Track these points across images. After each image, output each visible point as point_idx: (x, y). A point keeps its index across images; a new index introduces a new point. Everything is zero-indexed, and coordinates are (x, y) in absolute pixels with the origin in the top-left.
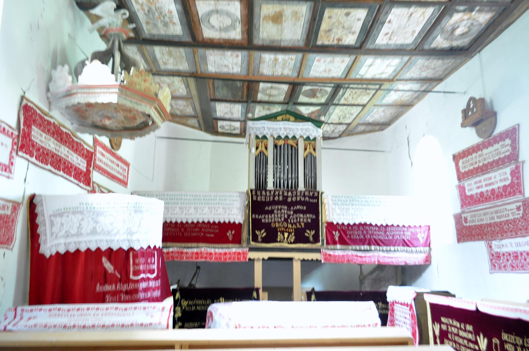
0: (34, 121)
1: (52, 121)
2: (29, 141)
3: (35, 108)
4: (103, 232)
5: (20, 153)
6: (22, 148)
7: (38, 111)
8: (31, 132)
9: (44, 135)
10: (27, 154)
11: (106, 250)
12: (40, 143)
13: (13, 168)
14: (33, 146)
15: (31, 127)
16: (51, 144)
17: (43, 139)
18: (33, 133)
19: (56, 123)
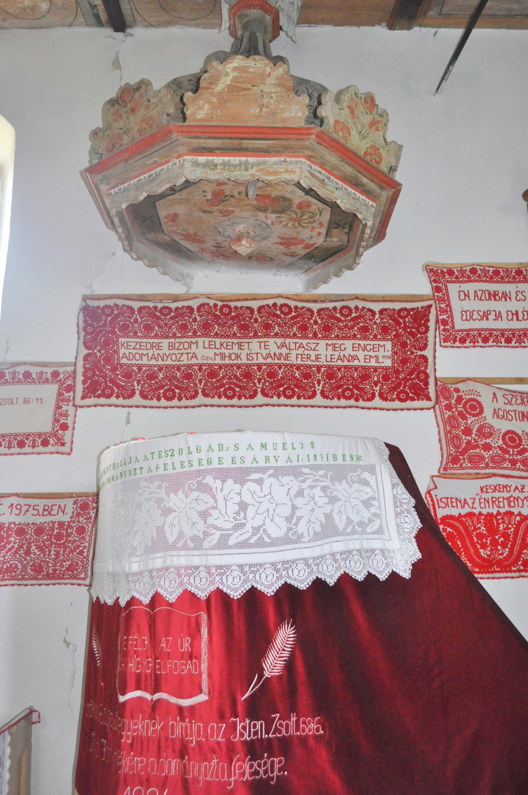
0: (125, 328)
1: (194, 304)
2: (114, 369)
3: (121, 302)
4: (349, 530)
5: (92, 401)
6: (93, 389)
7: (136, 305)
8: (116, 352)
9: (165, 342)
10: (108, 397)
11: (180, 598)
12: (153, 362)
13: (67, 436)
14: (128, 375)
15: (116, 343)
16: (204, 351)
17: (165, 350)
18: (122, 351)
19: (212, 303)
